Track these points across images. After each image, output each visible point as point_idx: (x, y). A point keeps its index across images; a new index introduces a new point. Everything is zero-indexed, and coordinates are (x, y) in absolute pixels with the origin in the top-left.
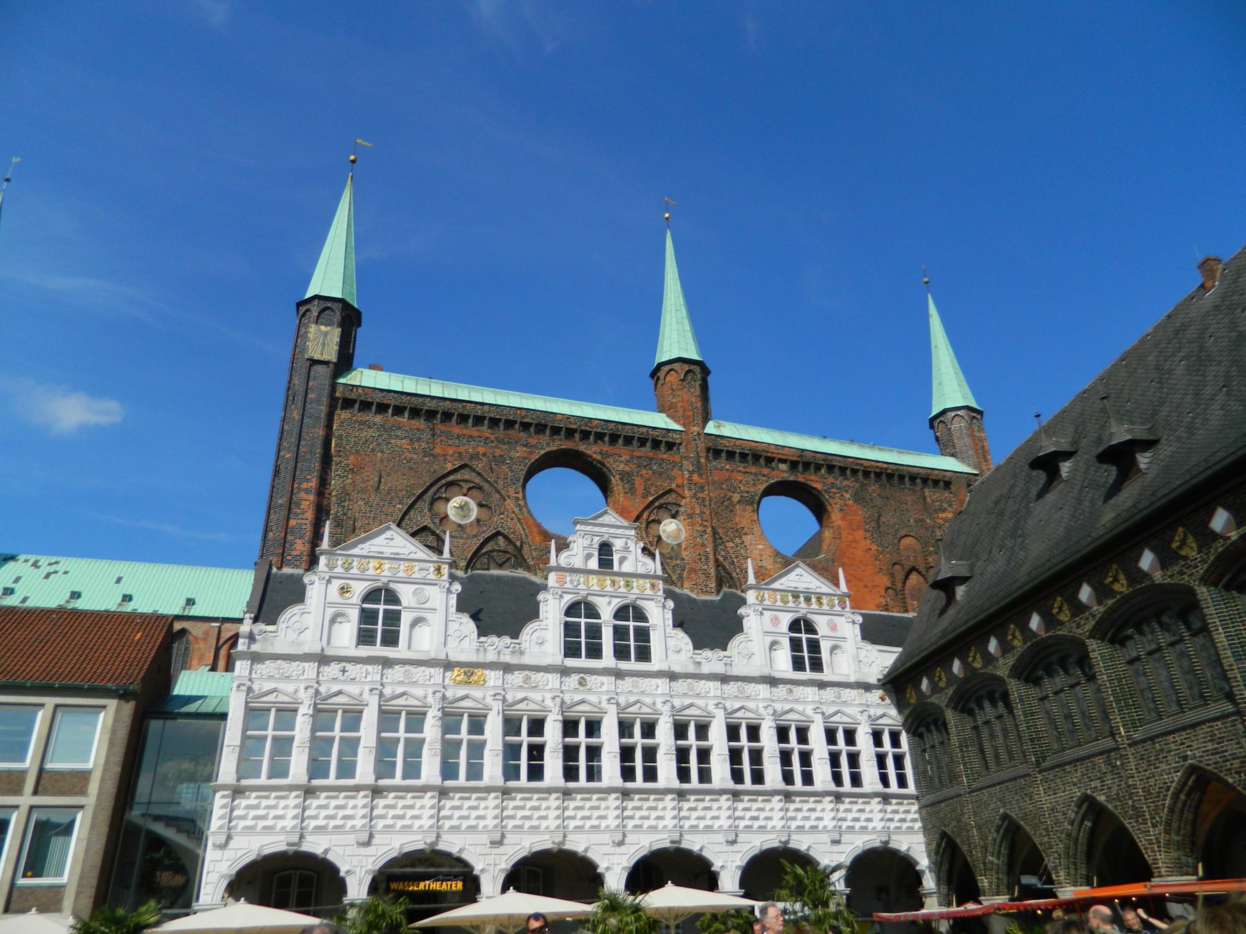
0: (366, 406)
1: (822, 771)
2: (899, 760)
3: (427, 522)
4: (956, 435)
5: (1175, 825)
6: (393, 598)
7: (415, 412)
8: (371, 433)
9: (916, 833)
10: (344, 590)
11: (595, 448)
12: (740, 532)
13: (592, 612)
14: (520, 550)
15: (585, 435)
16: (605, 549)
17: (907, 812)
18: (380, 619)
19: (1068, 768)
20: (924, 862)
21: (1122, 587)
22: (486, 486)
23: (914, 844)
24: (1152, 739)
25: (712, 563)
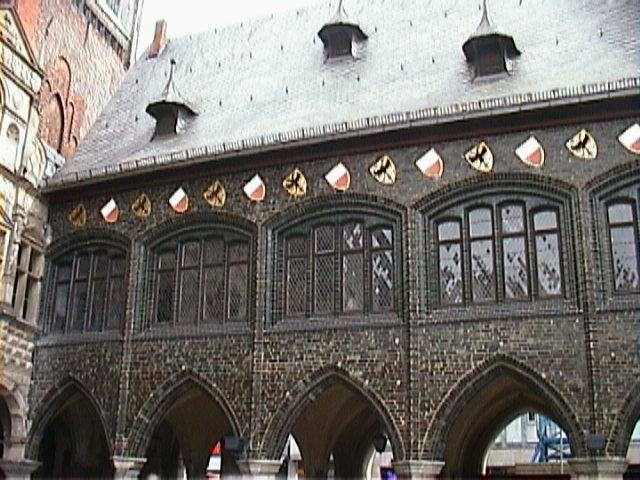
5: (448, 411)
9: (25, 371)
17: (24, 347)
19: (316, 336)
21: (487, 164)
24: (456, 323)
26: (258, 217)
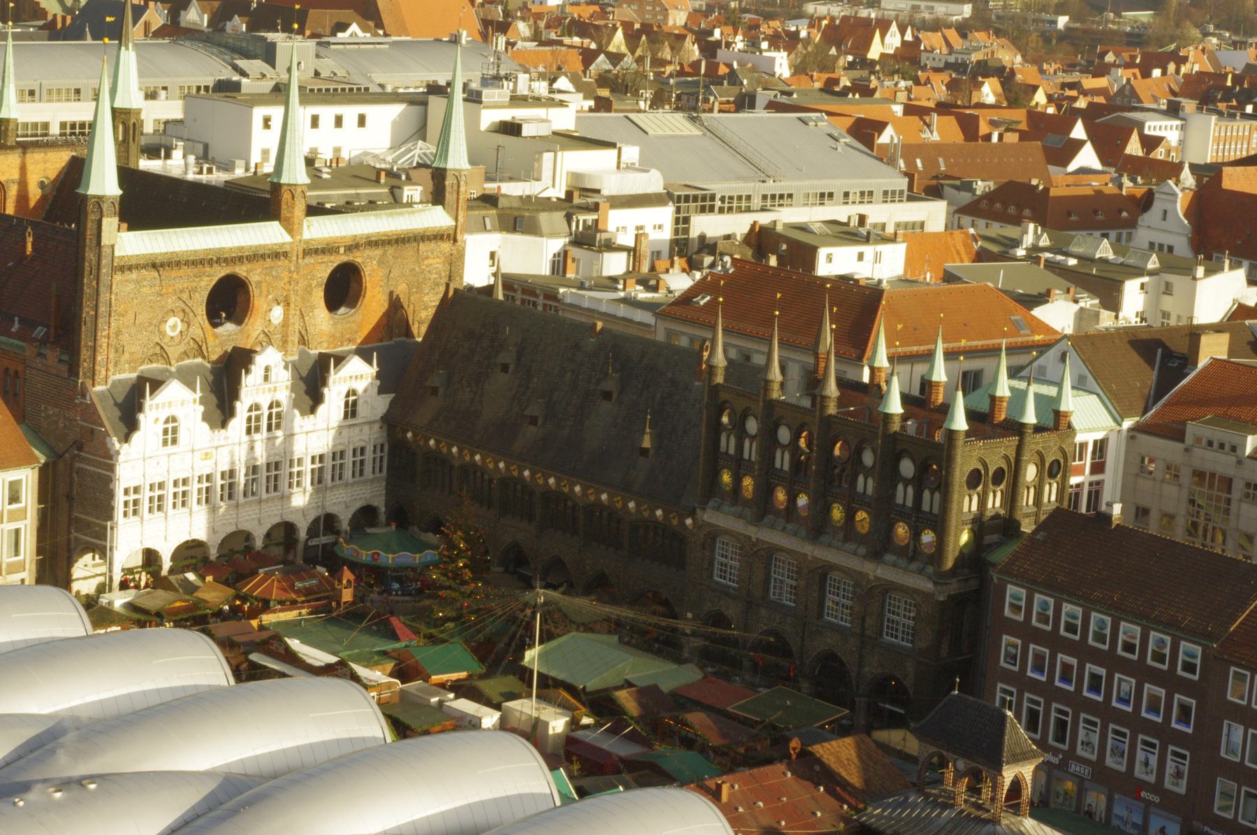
0: (130, 268)
1: (348, 473)
2: (381, 458)
3: (157, 340)
4: (448, 189)
6: (174, 419)
7: (154, 266)
8: (132, 286)
10: (157, 420)
11: (244, 268)
12: (312, 308)
13: (257, 407)
14: (200, 347)
15: (240, 259)
16: (267, 369)
18: (171, 435)
20: (383, 509)
22: (187, 310)
23: (380, 503)
25: (297, 334)
26: (456, 463)
